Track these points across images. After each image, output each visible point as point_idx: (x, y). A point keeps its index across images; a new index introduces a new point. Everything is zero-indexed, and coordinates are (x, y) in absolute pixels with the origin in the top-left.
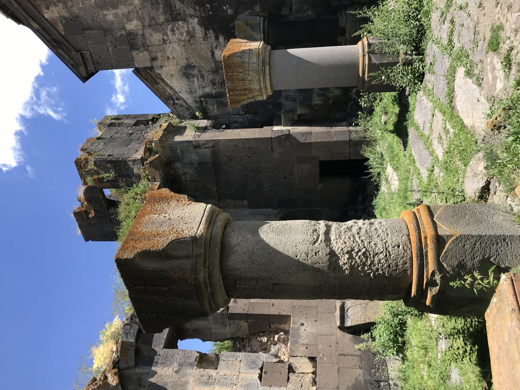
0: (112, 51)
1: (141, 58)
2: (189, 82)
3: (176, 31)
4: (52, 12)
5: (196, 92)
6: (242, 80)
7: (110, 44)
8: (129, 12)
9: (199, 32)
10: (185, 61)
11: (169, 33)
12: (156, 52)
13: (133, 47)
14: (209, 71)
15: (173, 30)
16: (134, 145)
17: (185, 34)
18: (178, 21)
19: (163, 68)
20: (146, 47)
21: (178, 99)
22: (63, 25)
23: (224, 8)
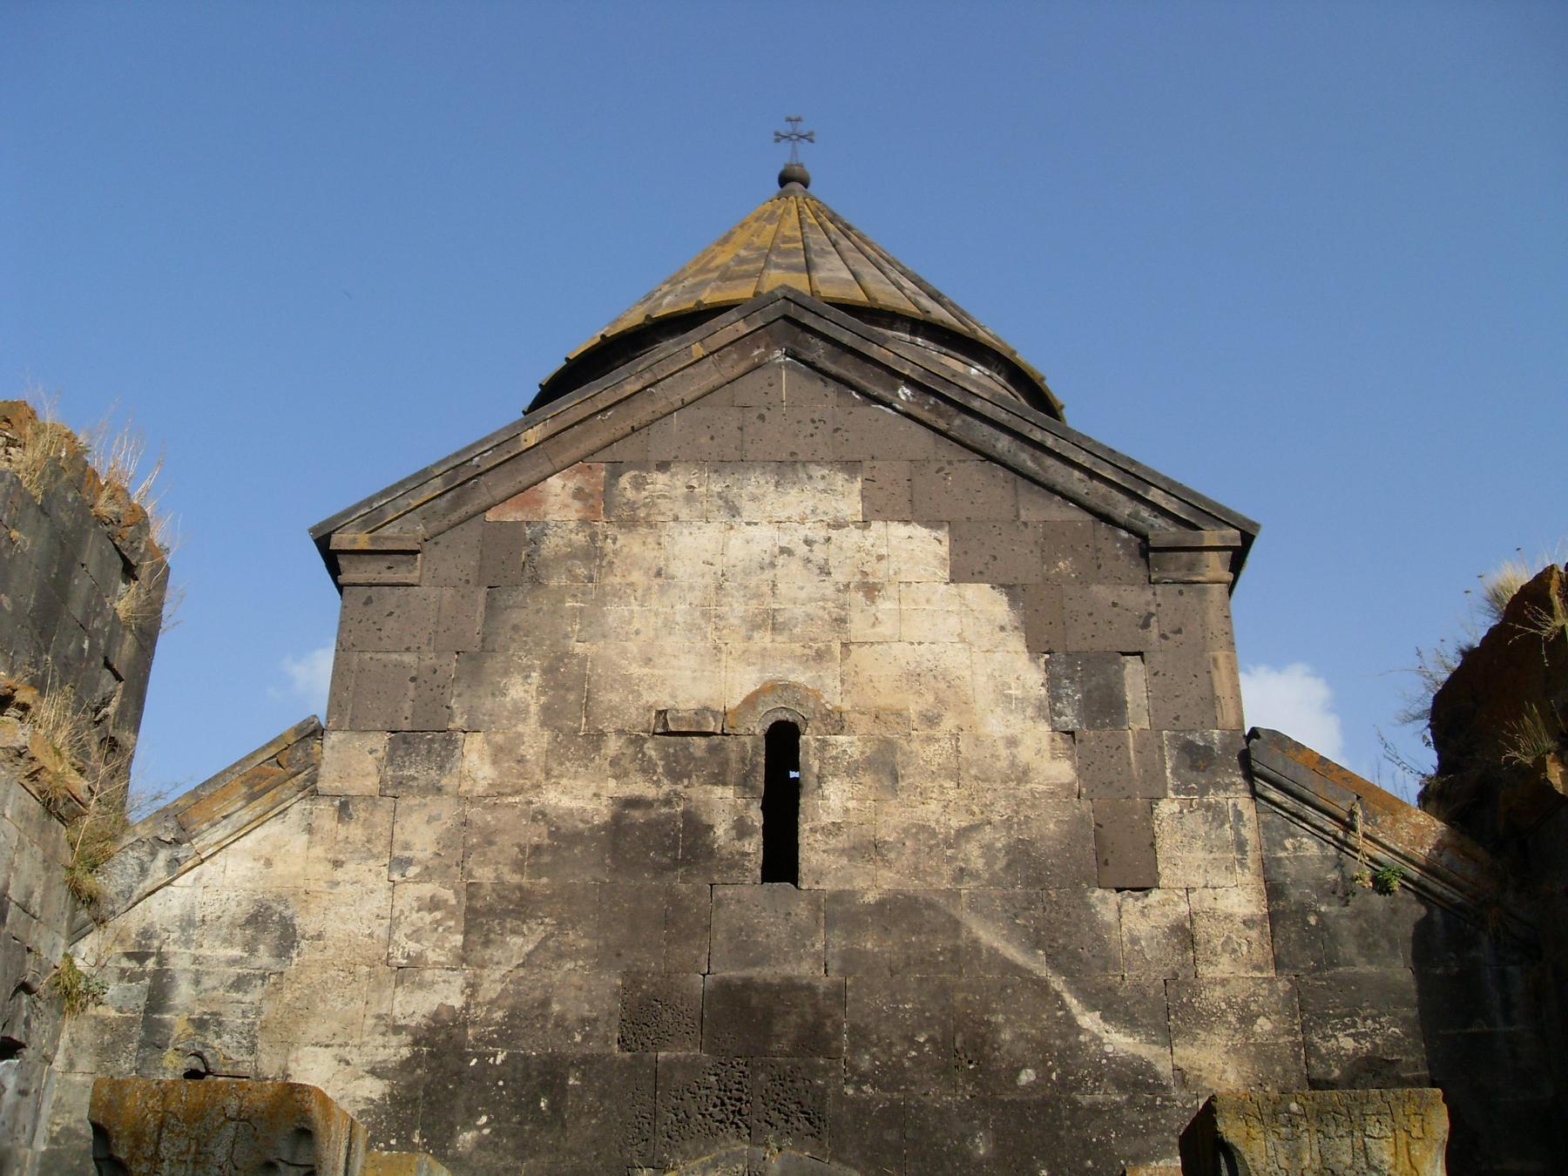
0: (401, 666)
1: (353, 761)
2: (232, 924)
3: (428, 918)
4: (566, 506)
5: (187, 943)
6: (199, 1153)
7: (428, 662)
8: (521, 761)
9: (415, 1006)
10: (311, 930)
11: (427, 889)
12: (367, 824)
13: (403, 741)
14: (259, 1013)
15: (434, 904)
17: (412, 947)
18: (466, 933)
19: (305, 837)
20: (394, 789)
21: (174, 862)
22: (517, 525)
23: (484, 1119)
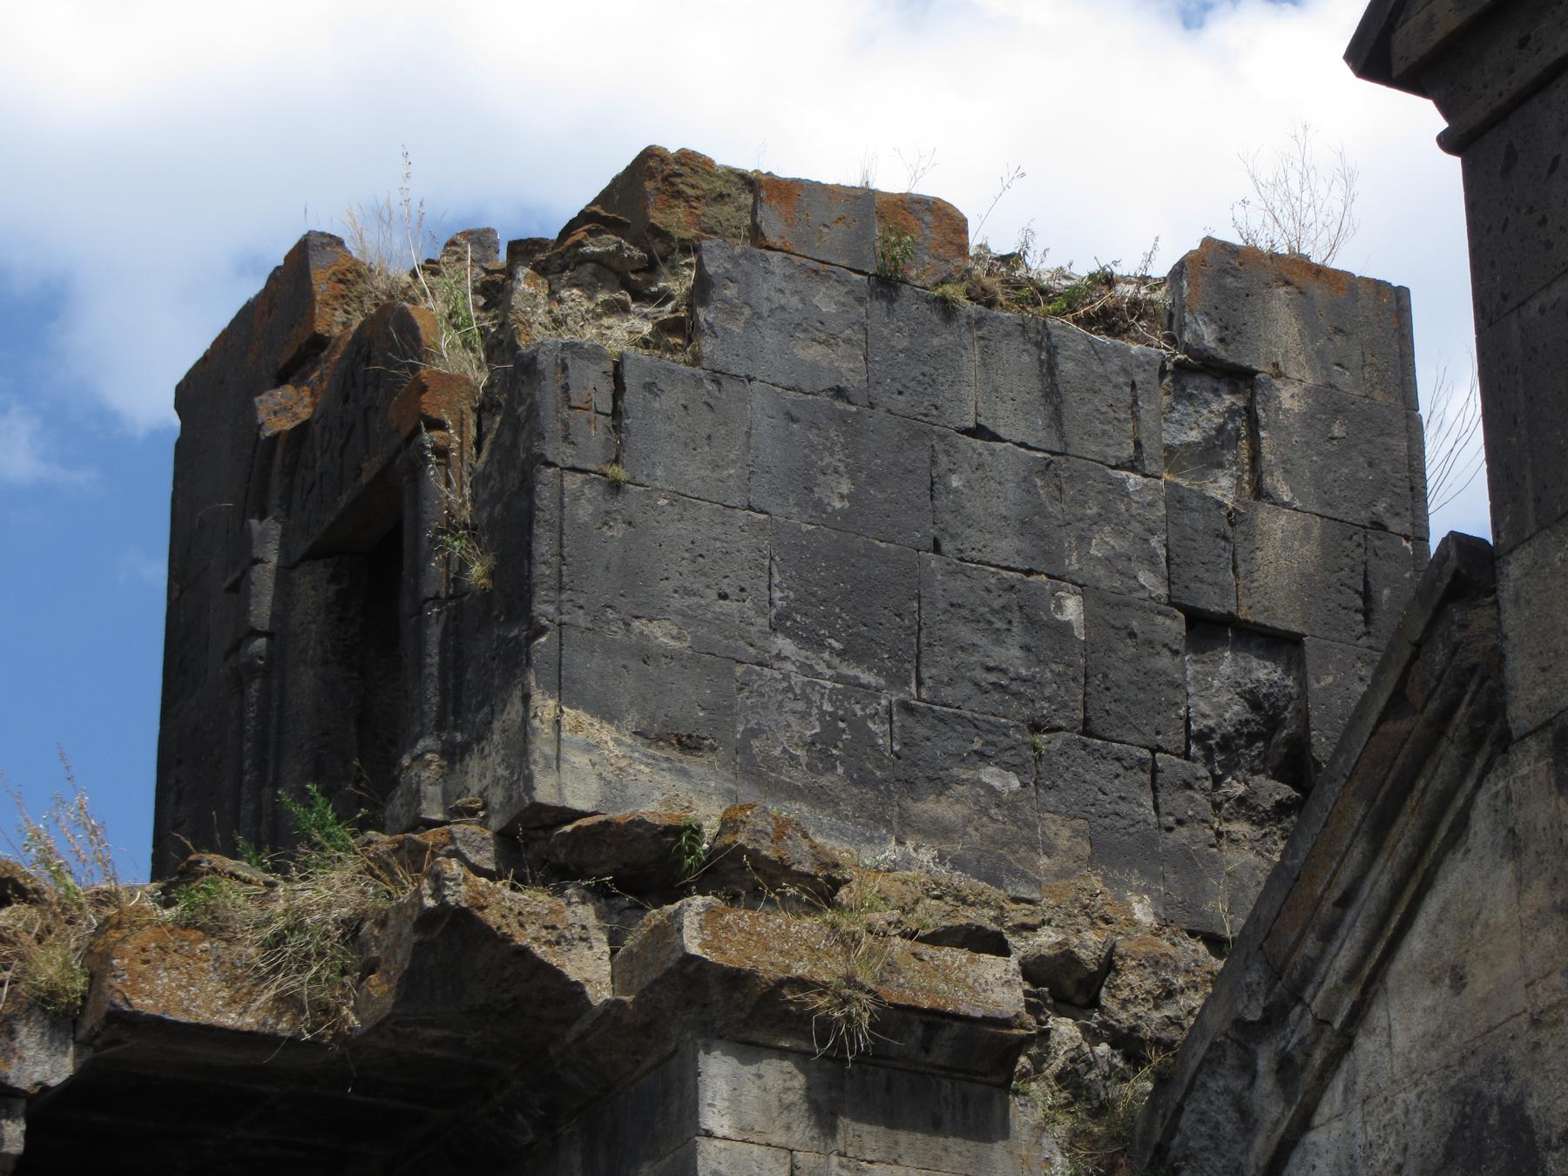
16: (798, 685)
19: (1507, 871)
